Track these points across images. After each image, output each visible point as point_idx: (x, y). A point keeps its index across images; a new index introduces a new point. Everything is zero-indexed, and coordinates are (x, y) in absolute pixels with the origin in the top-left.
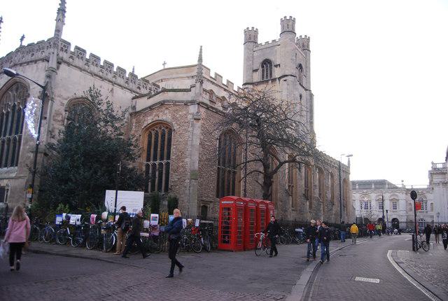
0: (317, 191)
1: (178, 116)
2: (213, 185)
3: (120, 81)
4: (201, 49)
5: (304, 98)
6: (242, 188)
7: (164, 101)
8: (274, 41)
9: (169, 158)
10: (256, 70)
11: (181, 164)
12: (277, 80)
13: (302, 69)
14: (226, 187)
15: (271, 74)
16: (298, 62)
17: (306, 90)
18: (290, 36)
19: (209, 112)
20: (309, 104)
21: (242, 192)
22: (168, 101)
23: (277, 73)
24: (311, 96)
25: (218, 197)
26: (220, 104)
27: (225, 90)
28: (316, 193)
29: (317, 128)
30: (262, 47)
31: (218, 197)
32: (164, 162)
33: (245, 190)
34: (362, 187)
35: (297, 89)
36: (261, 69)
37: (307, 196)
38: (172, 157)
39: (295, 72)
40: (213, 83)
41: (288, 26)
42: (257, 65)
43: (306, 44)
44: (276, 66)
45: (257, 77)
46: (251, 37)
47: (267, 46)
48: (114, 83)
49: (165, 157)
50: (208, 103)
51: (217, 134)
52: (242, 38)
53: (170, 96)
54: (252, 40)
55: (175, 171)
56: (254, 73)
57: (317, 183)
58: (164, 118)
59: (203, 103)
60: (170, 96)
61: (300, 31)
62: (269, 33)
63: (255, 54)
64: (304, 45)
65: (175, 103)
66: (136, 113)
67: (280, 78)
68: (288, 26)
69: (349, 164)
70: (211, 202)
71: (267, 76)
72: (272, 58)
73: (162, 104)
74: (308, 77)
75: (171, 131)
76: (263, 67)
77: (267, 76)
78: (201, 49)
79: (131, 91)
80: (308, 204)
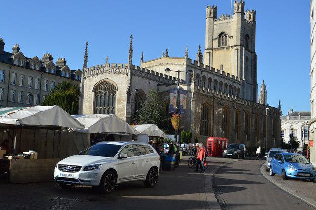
3: (152, 77)
5: (250, 60)
10: (216, 39)
16: (245, 33)
17: (252, 52)
23: (231, 42)
24: (255, 56)
29: (257, 82)
40: (193, 67)
42: (216, 36)
44: (230, 37)
45: (216, 44)
48: (150, 79)
66: (160, 93)
67: (232, 47)
69: (280, 106)
72: (227, 31)
79: (157, 81)
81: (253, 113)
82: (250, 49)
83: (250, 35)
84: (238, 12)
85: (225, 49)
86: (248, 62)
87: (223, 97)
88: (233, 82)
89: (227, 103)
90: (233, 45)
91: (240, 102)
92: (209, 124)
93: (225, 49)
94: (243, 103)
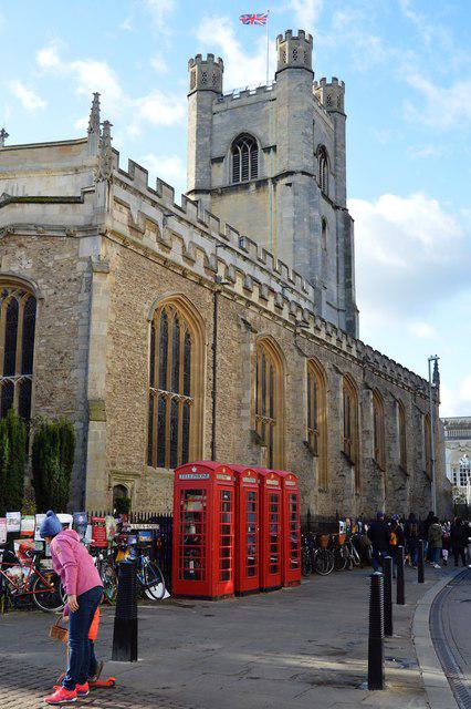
0: (370, 444)
1: (50, 264)
2: (140, 436)
4: (96, 103)
6: (206, 440)
7: (16, 227)
8: (261, 89)
9: (28, 367)
10: (219, 160)
11: (60, 384)
12: (269, 181)
13: (328, 158)
14: (168, 438)
15: (255, 169)
17: (336, 208)
18: (303, 78)
19: (128, 255)
20: (342, 240)
21: (206, 452)
22: (26, 227)
23: (269, 166)
25: (150, 463)
26: (153, 236)
27: (154, 203)
28: (368, 449)
30: (234, 104)
31: (150, 463)
32: (16, 379)
33: (213, 445)
34: (456, 433)
35: (314, 205)
36: (229, 157)
37: (350, 460)
38: (38, 365)
39: (310, 163)
41: (297, 54)
42: (222, 146)
43: (334, 99)
44: (267, 150)
45: (221, 175)
46: (207, 76)
47: (245, 100)
49: (18, 367)
50: (126, 231)
51: (145, 309)
52: (185, 81)
53: (31, 212)
54: (210, 85)
55: (46, 402)
56: (216, 165)
57: (371, 427)
58: (15, 268)
59: (113, 232)
60: (31, 212)
61: (323, 66)
62: (249, 70)
63: (217, 120)
64: (334, 102)
65: (43, 232)
67: (275, 179)
68: (297, 54)
69: (436, 375)
70: (137, 475)
71: (245, 174)
73: (9, 234)
74: (341, 179)
75: (32, 303)
76: (235, 151)
77: (245, 174)
78: (96, 103)
80: (353, 472)
81: (368, 387)
82: (332, 195)
83: (330, 151)
84: (294, 64)
85: (253, 187)
86: (328, 237)
87: (255, 298)
88: (285, 286)
89: (271, 329)
90: (278, 172)
91: (322, 336)
92: (193, 411)
93: (253, 187)
94: (333, 342)
